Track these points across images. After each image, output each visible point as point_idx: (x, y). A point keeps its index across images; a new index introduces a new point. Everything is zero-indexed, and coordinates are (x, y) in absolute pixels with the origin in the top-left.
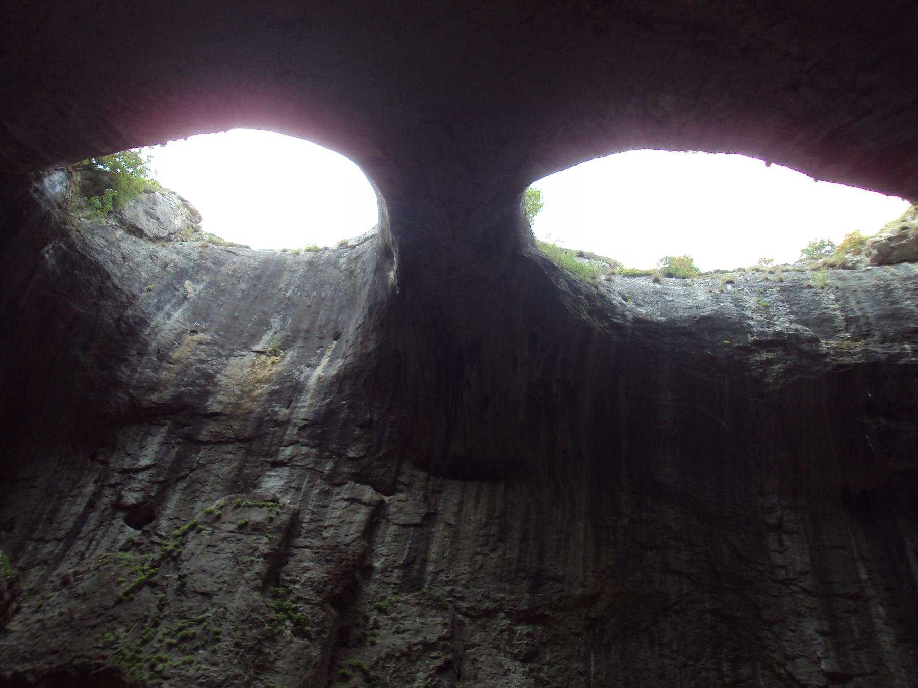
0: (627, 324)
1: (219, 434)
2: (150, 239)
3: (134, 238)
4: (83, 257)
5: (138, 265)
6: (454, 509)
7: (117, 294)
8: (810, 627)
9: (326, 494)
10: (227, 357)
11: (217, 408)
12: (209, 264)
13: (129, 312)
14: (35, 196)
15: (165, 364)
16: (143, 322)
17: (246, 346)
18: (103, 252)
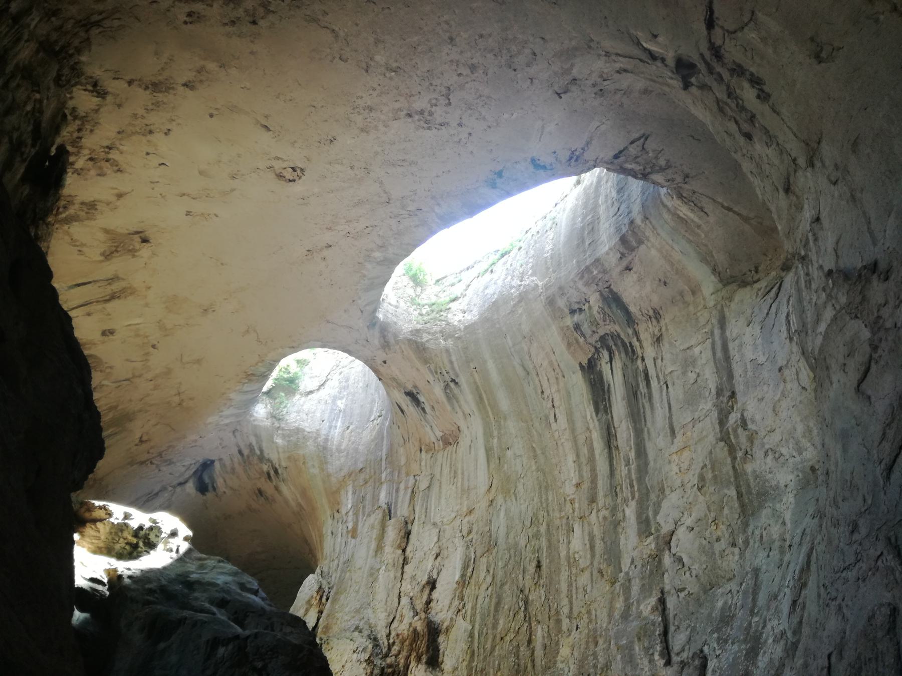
0: (462, 333)
1: (365, 479)
2: (318, 390)
3: (310, 396)
4: (289, 430)
5: (314, 412)
6: (439, 469)
7: (311, 435)
8: (571, 458)
9: (397, 490)
10: (362, 433)
11: (360, 466)
12: (344, 384)
13: (320, 439)
14: (256, 423)
15: (342, 454)
16: (326, 440)
17: (368, 421)
18: (297, 420)
